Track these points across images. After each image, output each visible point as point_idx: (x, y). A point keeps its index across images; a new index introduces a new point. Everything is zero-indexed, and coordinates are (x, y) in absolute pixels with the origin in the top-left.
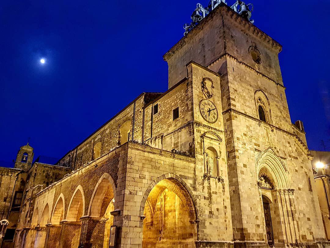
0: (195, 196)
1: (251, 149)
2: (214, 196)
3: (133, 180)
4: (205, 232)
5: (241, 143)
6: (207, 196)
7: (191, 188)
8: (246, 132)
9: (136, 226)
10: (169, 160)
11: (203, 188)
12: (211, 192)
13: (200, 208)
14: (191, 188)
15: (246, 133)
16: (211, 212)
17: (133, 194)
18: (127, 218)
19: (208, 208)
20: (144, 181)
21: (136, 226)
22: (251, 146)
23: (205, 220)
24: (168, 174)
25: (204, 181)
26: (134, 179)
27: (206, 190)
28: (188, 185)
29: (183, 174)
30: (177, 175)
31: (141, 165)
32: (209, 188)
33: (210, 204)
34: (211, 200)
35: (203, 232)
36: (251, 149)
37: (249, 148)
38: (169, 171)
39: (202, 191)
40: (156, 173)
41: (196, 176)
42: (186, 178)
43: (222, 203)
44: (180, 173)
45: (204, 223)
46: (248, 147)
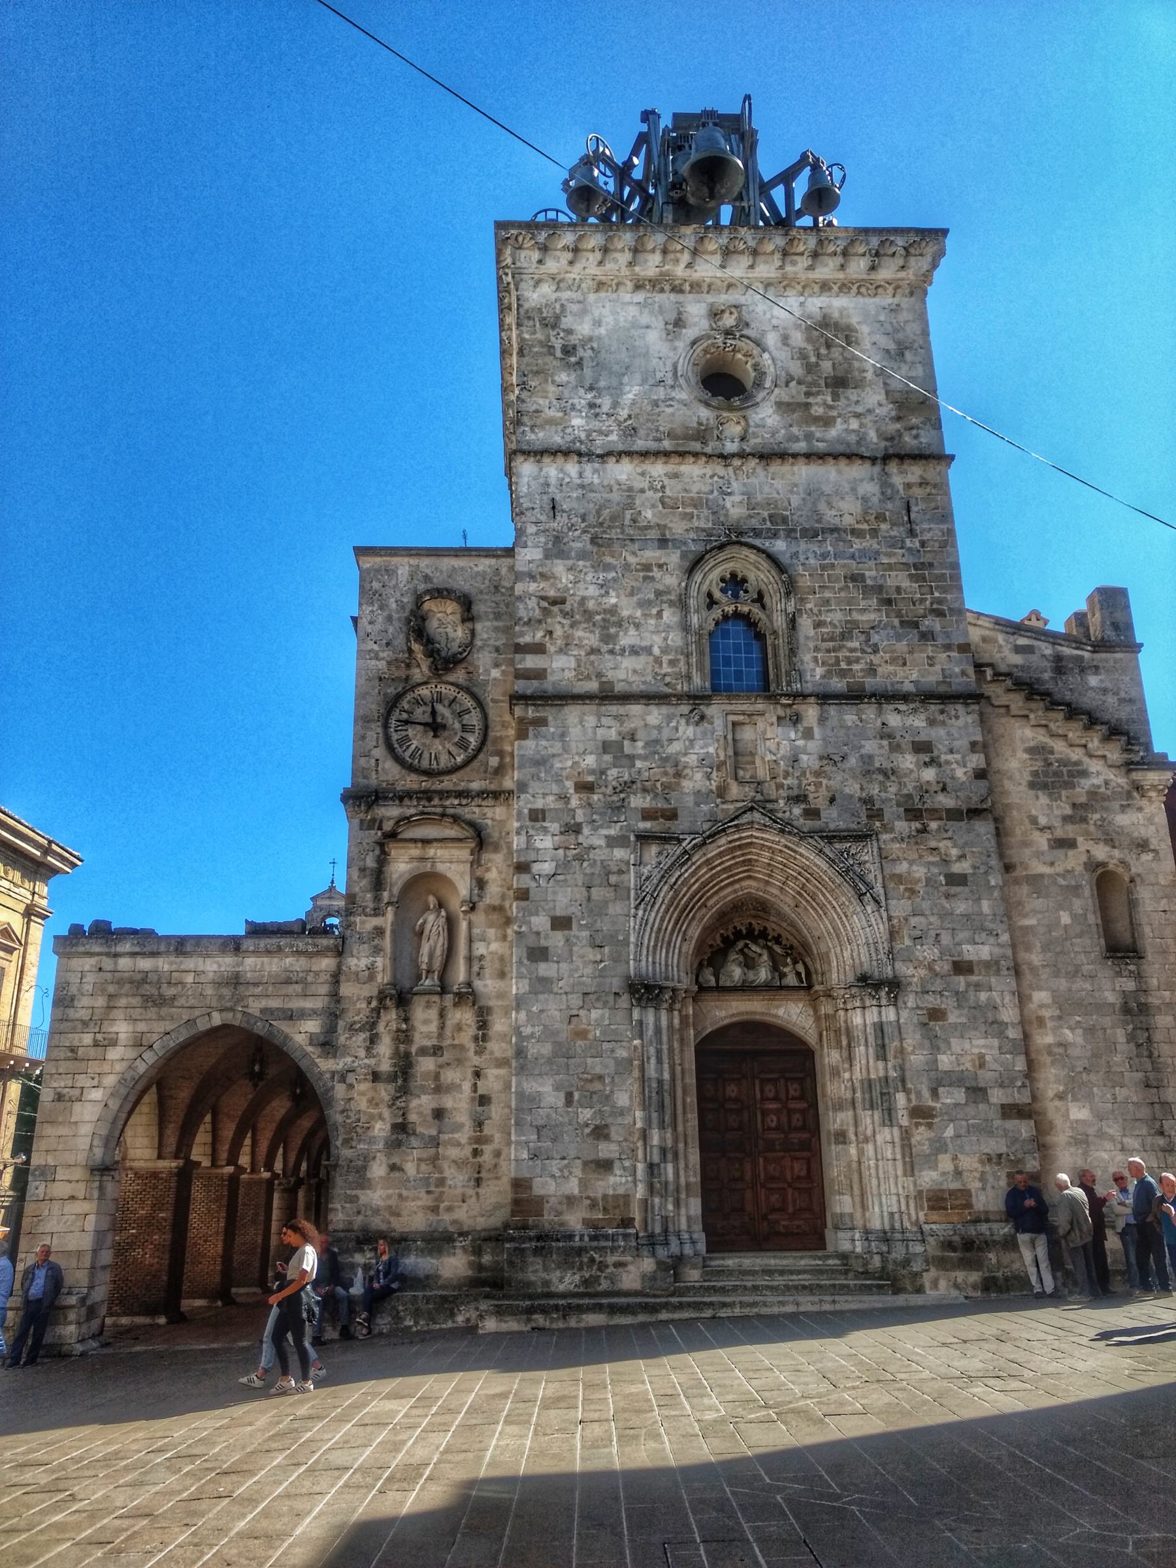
0: (328, 1076)
1: (612, 842)
2: (426, 1064)
3: (70, 1054)
4: (361, 1202)
5: (554, 827)
6: (386, 1066)
7: (310, 1049)
8: (592, 772)
9: (72, 1198)
10: (219, 966)
11: (373, 1040)
12: (413, 1050)
13: (348, 1117)
14: (310, 1049)
15: (591, 778)
16: (402, 1128)
17: (67, 1098)
18: (43, 1174)
19: (386, 1113)
20: (114, 1054)
21: (72, 1198)
22: (613, 831)
23: (367, 1158)
24: (209, 1014)
25: (379, 1013)
26: (72, 1051)
27: (385, 1048)
28: (300, 1039)
29: (274, 1003)
30: (250, 1011)
31: (100, 1002)
32: (404, 1036)
33: (397, 1098)
34: (405, 1080)
35: (351, 1202)
36: (612, 842)
37: (602, 842)
38: (214, 1004)
39: (362, 1053)
40: (161, 1018)
41: (338, 1002)
42: (291, 1016)
43: (467, 1086)
44: (264, 1003)
45: (362, 1170)
46: (589, 837)
